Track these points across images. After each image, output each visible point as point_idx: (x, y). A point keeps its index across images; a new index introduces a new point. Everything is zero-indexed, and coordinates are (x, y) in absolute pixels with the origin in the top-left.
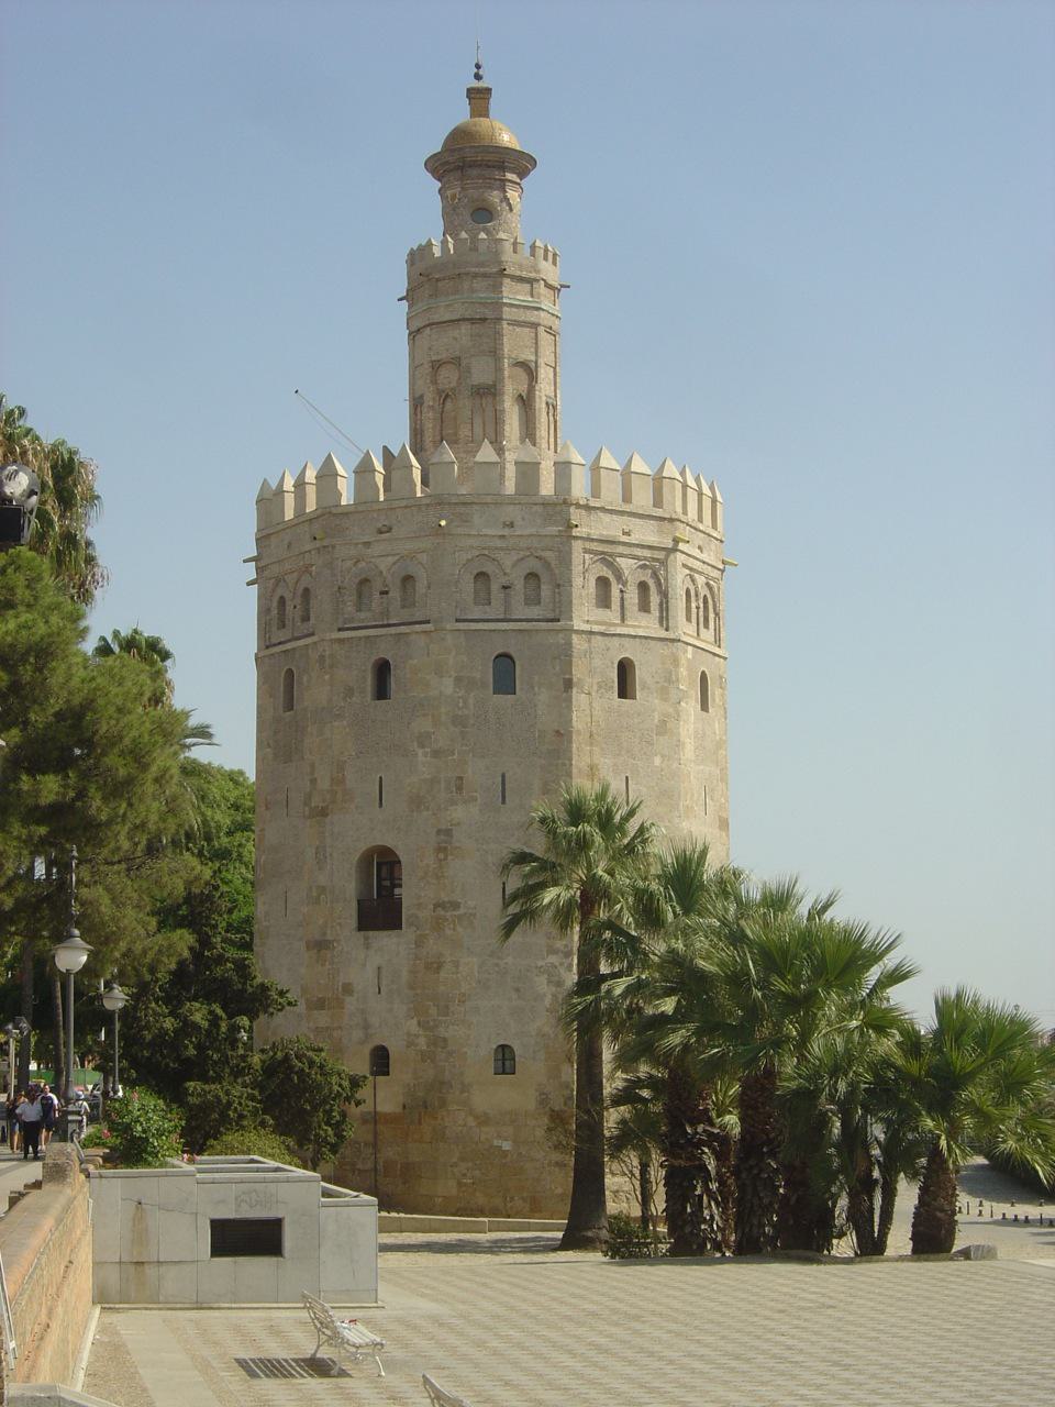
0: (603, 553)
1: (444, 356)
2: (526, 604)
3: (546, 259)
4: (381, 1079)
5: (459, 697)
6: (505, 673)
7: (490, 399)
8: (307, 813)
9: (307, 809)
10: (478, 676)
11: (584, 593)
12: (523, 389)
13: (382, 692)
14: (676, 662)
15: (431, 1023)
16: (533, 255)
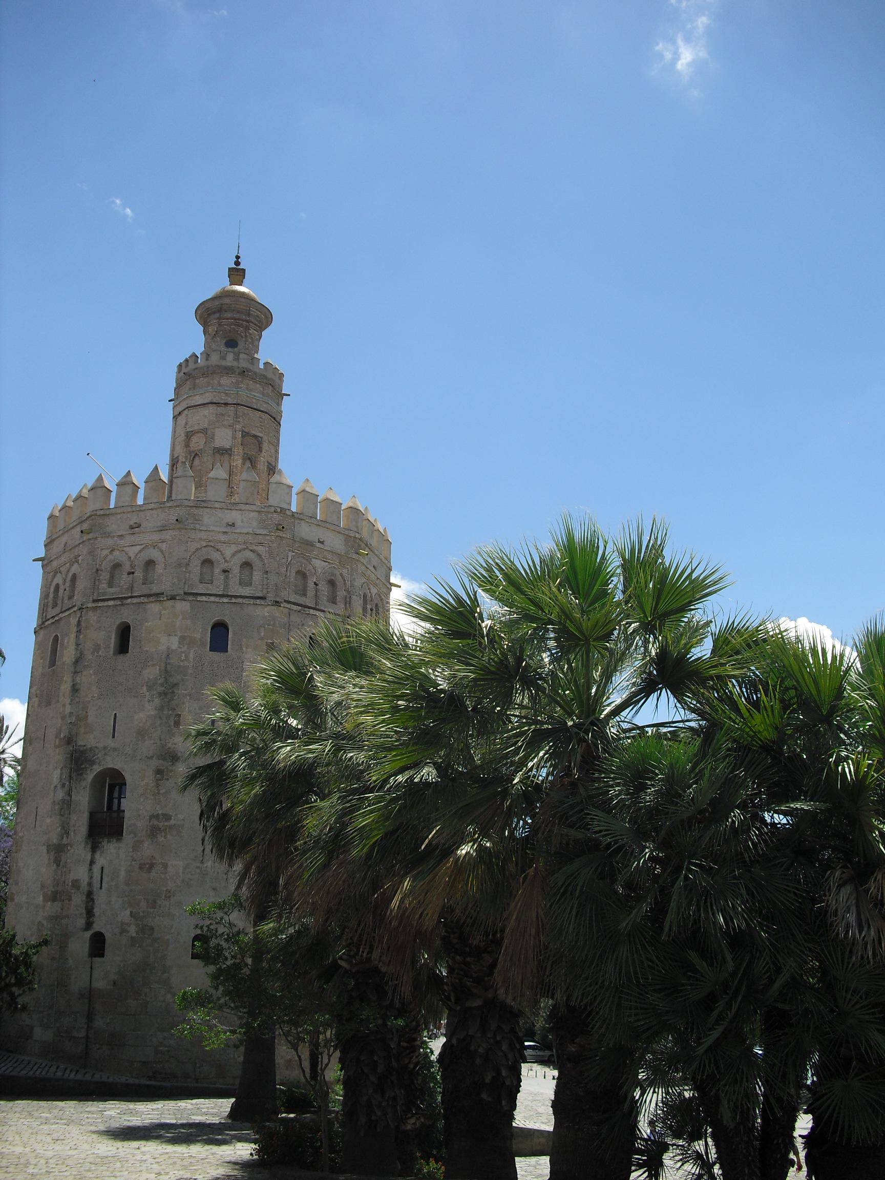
1: (196, 428)
2: (240, 584)
4: (97, 960)
5: (182, 652)
6: (219, 636)
7: (226, 457)
8: (57, 743)
9: (57, 741)
10: (198, 636)
15: (141, 914)
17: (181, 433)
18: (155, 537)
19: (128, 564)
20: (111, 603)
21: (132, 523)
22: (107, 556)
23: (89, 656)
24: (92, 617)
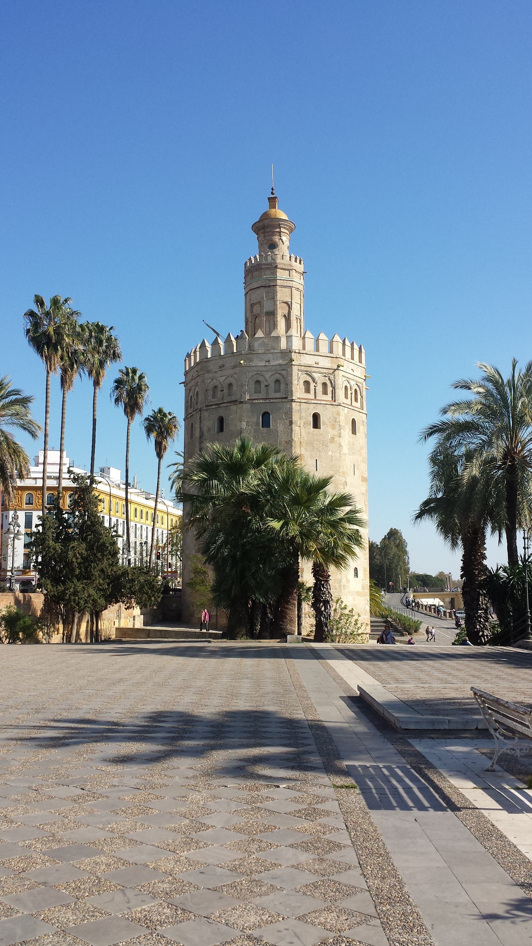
0: (307, 371)
1: (255, 302)
3: (296, 261)
7: (272, 316)
11: (298, 387)
12: (286, 312)
13: (221, 429)
14: (338, 414)
16: (290, 260)
17: (248, 304)
18: (231, 371)
19: (220, 386)
20: (214, 407)
21: (220, 365)
22: (210, 382)
23: (205, 432)
24: (206, 414)
